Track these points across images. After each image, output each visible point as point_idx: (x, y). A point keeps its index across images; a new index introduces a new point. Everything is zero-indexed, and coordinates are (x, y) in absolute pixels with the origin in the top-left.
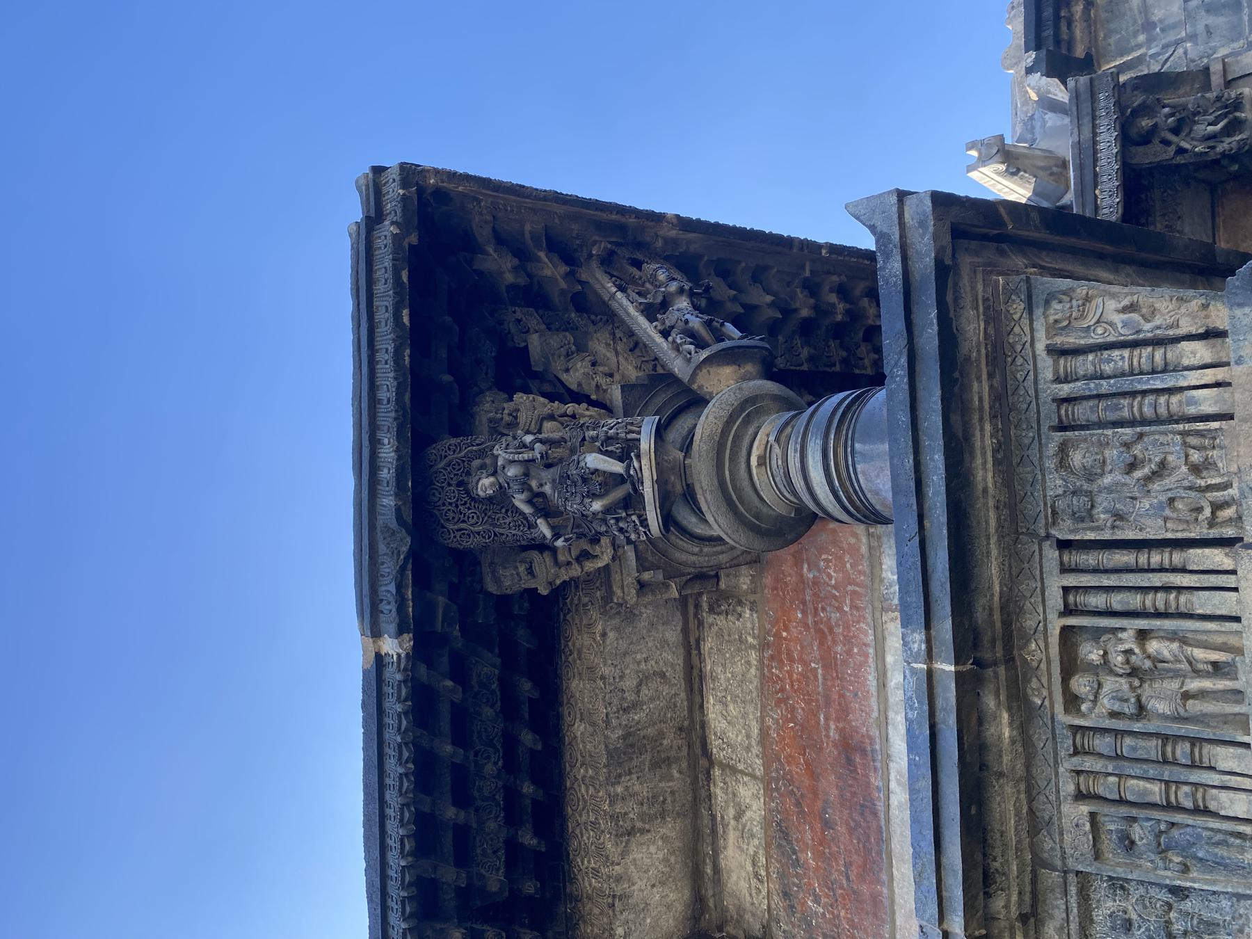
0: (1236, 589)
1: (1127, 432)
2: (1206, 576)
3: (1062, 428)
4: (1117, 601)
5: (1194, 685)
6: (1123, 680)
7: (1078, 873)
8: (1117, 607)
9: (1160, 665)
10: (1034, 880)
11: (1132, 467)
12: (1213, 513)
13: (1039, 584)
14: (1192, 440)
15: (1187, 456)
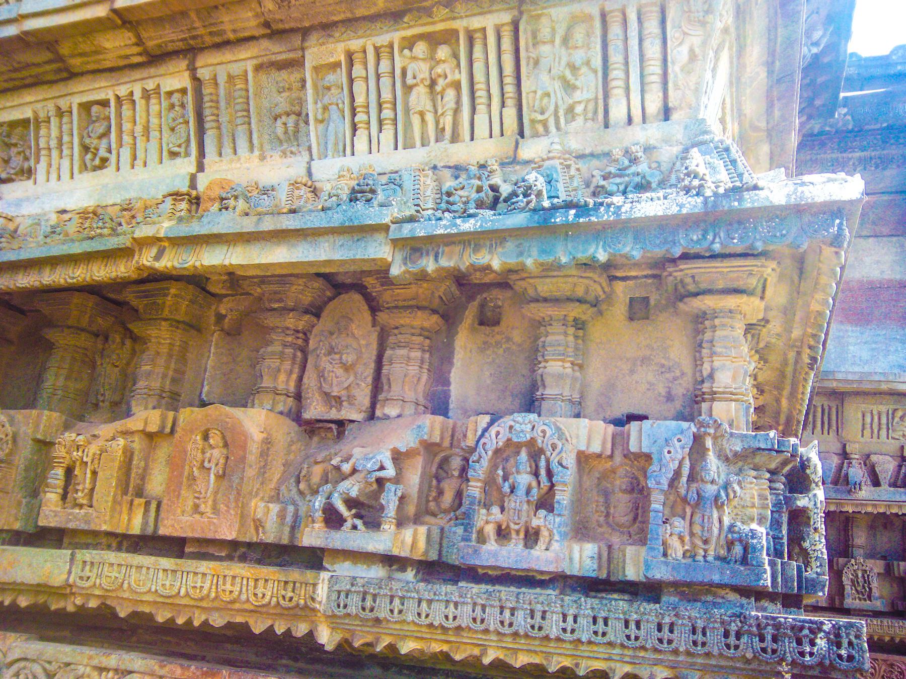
0: (491, 137)
1: (597, 62)
2: (498, 120)
3: (603, 16)
4: (478, 67)
5: (430, 118)
6: (427, 75)
7: (303, 57)
8: (475, 65)
9: (439, 97)
10: (292, 30)
11: (573, 68)
12: (540, 121)
13: (485, 10)
14: (591, 107)
15: (580, 102)
